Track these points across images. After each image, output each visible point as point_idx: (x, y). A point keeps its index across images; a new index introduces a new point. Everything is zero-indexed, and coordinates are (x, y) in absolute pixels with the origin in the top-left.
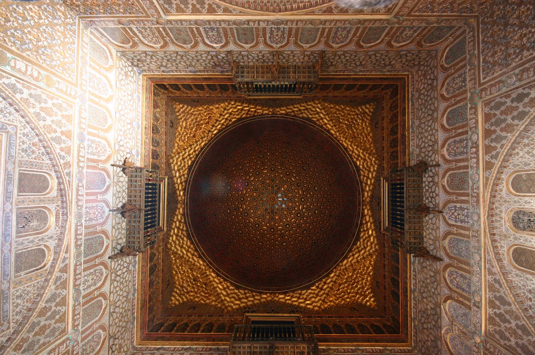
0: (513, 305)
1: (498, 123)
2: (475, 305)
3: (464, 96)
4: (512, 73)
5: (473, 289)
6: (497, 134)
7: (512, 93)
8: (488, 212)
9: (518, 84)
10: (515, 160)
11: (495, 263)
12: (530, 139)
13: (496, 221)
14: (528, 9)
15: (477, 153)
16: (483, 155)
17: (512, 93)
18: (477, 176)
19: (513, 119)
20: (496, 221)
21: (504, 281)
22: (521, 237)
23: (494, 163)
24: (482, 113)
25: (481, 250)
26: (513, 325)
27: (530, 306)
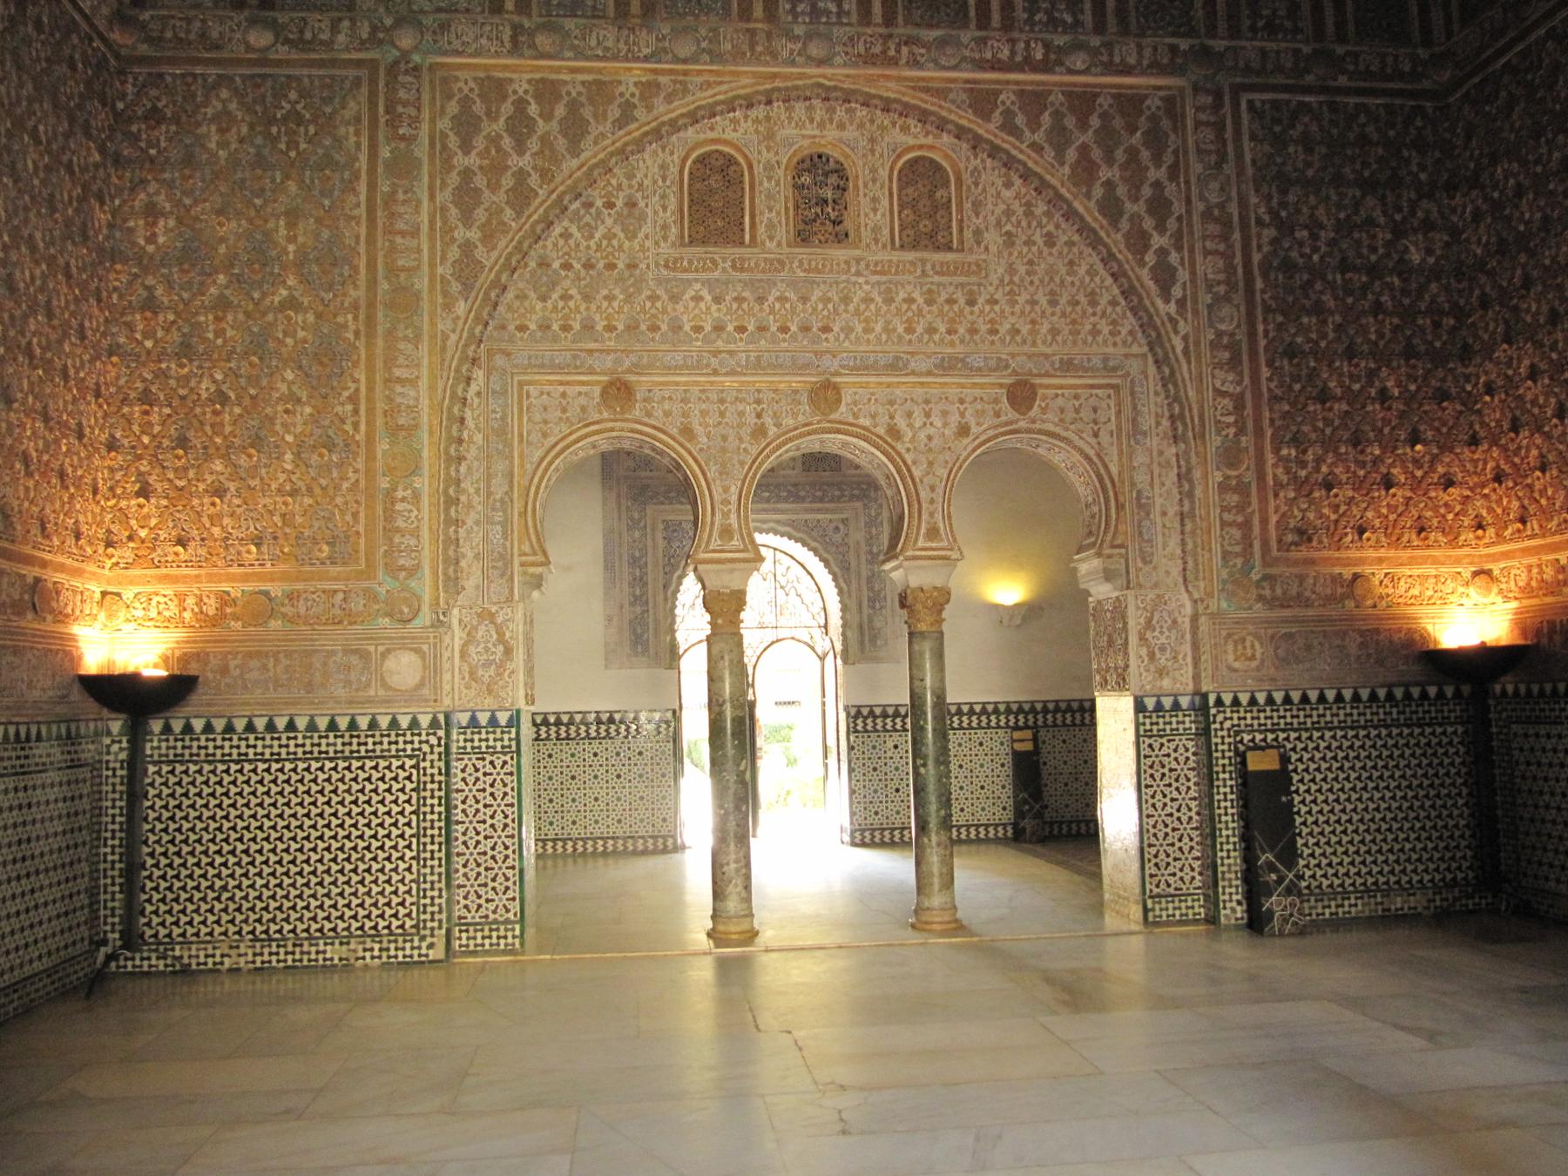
0: (575, 163)
1: (1107, 137)
2: (517, 29)
3: (1222, 25)
4: (1234, 194)
5: (569, 24)
6: (1076, 133)
7: (1178, 184)
8: (835, 88)
9: (1199, 206)
10: (992, 175)
11: (680, 107)
12: (1045, 220)
13: (810, 108)
14: (1374, 249)
15: (1028, 64)
16: (1017, 83)
17: (1178, 184)
18: (953, 62)
19: (1109, 184)
20: (810, 108)
21: (637, 134)
22: (778, 184)
23: (989, 120)
24: (1147, 87)
25: (712, 62)
26: (516, 162)
27: (591, 205)
